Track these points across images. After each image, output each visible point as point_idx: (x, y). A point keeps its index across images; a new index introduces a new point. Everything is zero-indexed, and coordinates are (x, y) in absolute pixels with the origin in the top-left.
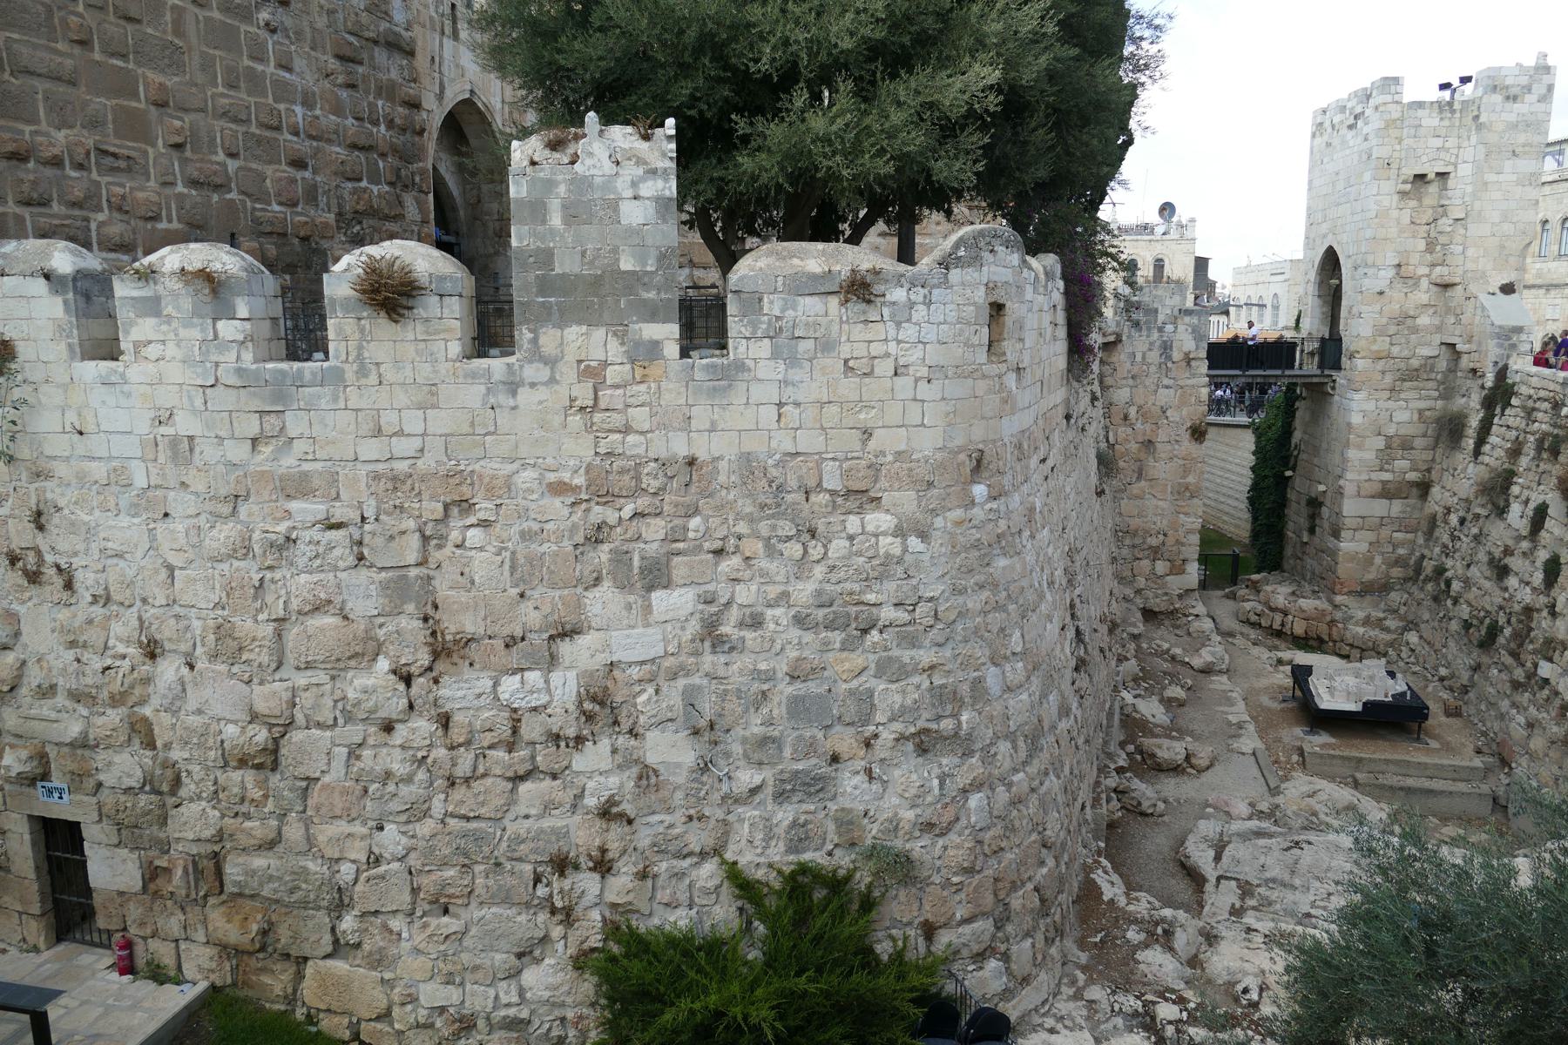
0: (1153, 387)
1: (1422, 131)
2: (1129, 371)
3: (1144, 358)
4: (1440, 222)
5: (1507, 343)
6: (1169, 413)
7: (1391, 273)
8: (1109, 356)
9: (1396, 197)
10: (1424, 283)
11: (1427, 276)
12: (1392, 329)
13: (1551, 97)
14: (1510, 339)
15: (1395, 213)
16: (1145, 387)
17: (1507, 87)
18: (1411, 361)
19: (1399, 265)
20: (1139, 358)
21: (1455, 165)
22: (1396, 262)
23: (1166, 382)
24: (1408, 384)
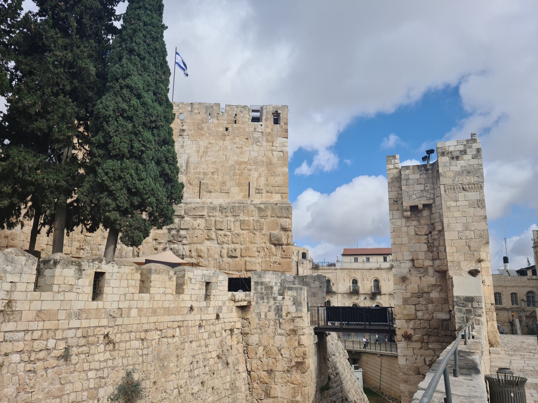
0: (272, 335)
1: (410, 182)
2: (258, 324)
3: (266, 316)
4: (433, 233)
5: (464, 309)
6: (282, 352)
7: (409, 264)
8: (246, 315)
9: (404, 220)
10: (431, 271)
11: (432, 266)
12: (415, 300)
13: (480, 155)
14: (467, 306)
15: (405, 229)
16: (268, 334)
17: (451, 152)
18: (432, 322)
19: (413, 260)
20: (263, 316)
21: (434, 199)
22: (410, 258)
23: (279, 331)
24: (432, 339)
